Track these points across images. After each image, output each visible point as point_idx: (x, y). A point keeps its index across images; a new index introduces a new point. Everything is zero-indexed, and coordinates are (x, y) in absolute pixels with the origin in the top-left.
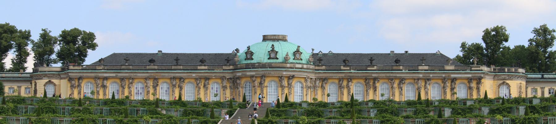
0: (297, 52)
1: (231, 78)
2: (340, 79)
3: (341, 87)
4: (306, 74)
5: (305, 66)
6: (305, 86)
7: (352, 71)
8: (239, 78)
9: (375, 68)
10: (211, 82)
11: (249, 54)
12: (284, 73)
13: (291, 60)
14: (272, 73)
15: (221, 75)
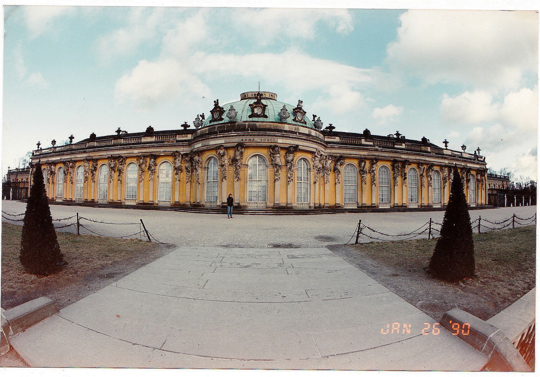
0: (298, 110)
1: (186, 155)
2: (361, 158)
3: (362, 171)
4: (315, 146)
5: (313, 133)
6: (312, 166)
7: (377, 147)
8: (200, 152)
9: (403, 146)
10: (159, 161)
11: (217, 110)
12: (280, 141)
13: (290, 120)
14: (257, 139)
15: (174, 149)
